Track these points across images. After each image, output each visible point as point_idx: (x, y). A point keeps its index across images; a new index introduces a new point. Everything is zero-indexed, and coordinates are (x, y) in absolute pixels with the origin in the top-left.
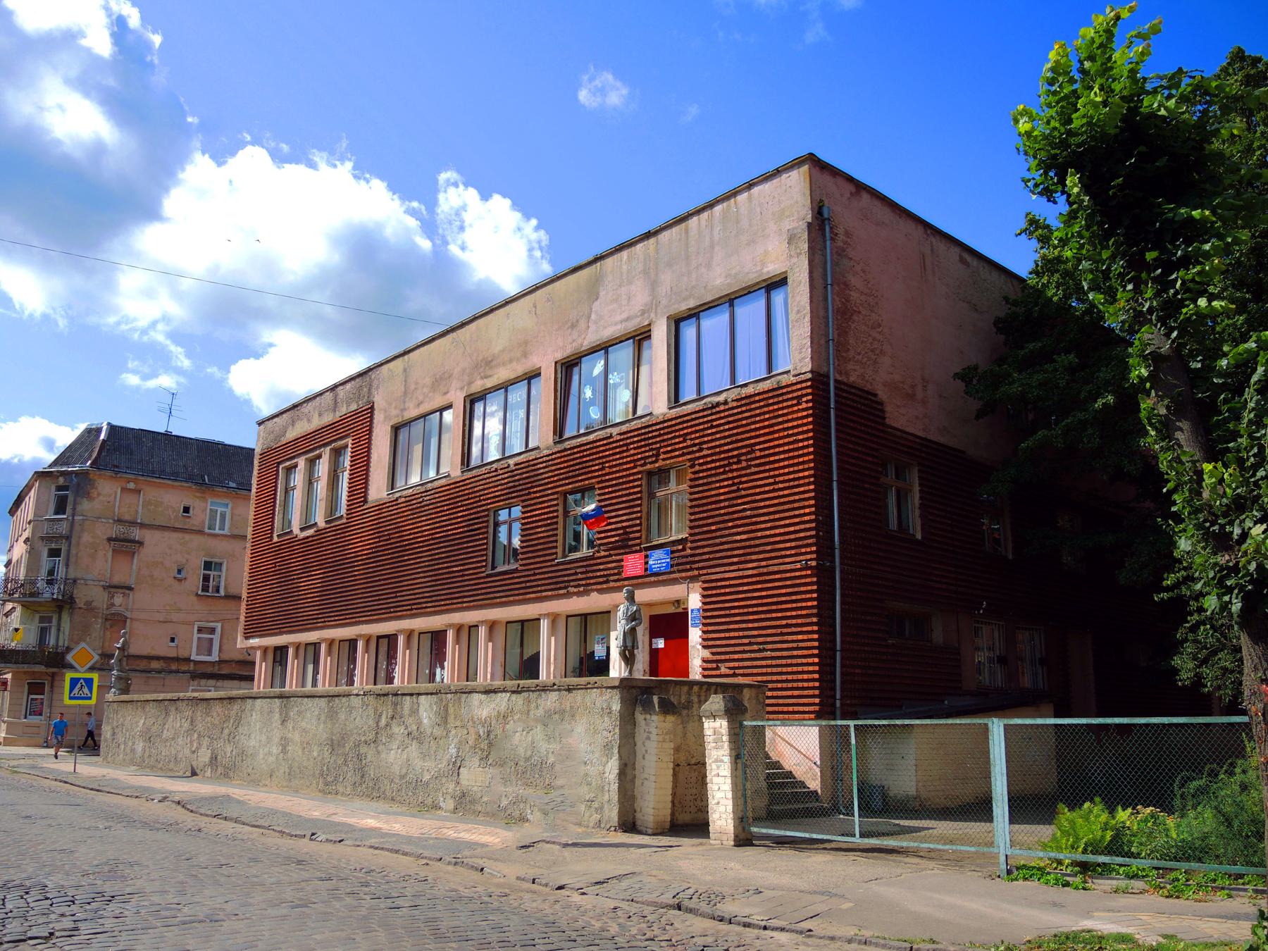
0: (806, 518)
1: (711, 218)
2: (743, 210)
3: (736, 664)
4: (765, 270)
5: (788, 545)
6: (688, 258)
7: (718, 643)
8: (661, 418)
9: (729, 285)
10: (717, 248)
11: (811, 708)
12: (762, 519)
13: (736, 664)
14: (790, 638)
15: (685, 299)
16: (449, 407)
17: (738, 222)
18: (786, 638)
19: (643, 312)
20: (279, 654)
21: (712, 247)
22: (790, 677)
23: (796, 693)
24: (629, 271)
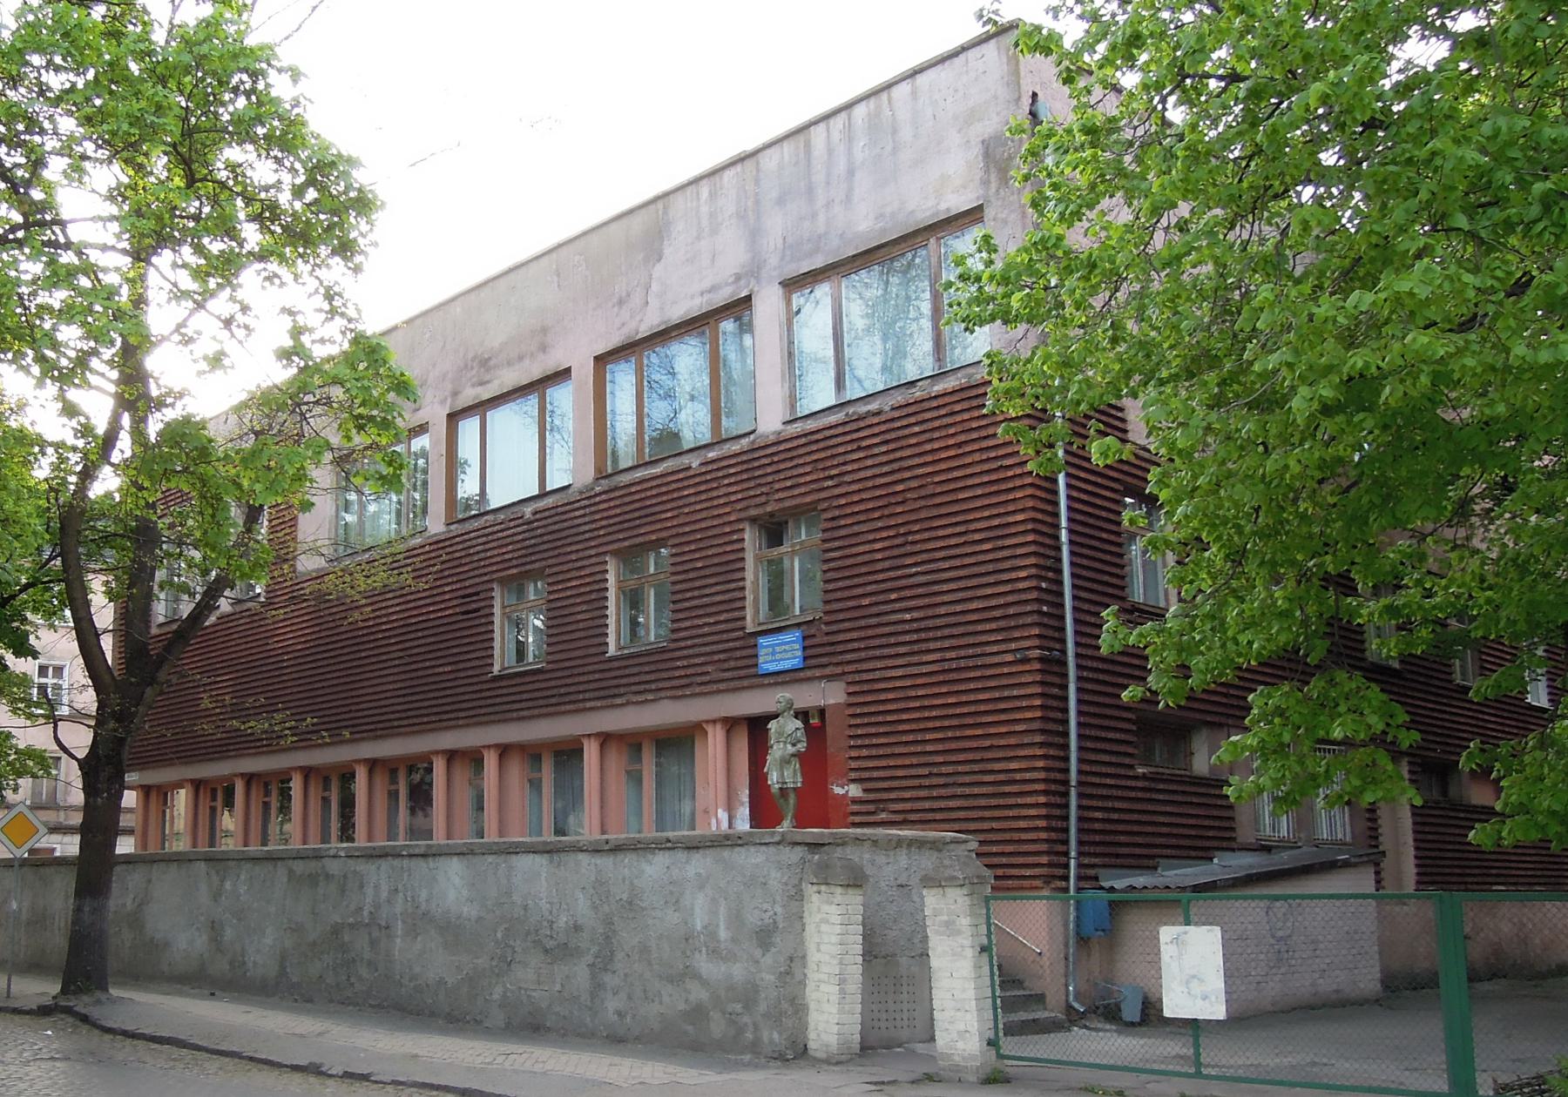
0: (1021, 585)
1: (849, 126)
2: (903, 114)
3: (908, 806)
4: (943, 206)
5: (988, 627)
6: (810, 191)
7: (875, 774)
8: (772, 438)
9: (883, 231)
10: (858, 175)
11: (1037, 871)
12: (945, 587)
13: (908, 806)
14: (997, 766)
15: (810, 255)
16: (563, 375)
17: (895, 132)
18: (989, 766)
19: (738, 278)
20: (474, 758)
21: (851, 172)
22: (995, 825)
23: (1009, 848)
24: (712, 215)
